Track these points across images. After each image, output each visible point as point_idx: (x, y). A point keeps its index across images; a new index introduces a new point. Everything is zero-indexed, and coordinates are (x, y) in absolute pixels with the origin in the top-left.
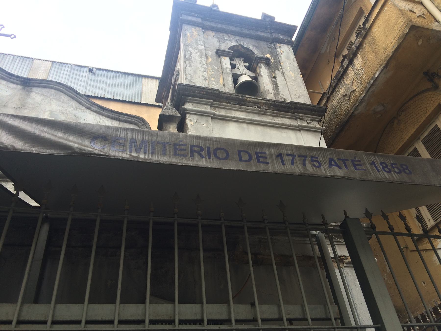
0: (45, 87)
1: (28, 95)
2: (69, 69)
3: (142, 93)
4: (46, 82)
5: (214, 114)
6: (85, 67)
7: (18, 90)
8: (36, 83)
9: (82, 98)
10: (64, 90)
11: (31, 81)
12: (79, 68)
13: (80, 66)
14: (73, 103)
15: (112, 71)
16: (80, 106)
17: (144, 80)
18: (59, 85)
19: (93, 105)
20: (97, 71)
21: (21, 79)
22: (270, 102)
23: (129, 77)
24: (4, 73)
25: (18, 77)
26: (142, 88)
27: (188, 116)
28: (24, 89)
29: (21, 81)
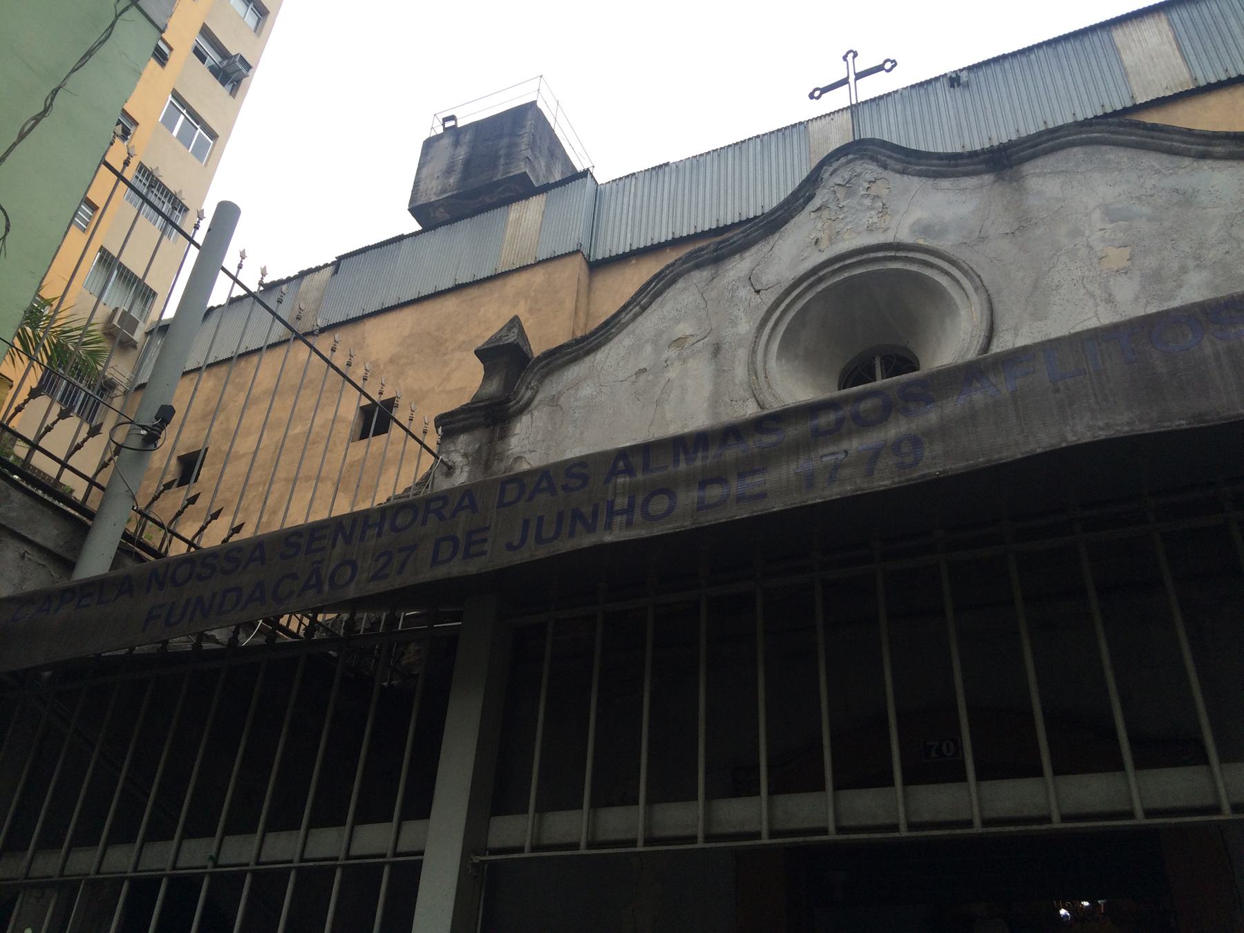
0: (1053, 150)
2: (899, 107)
3: (1125, 75)
4: (1050, 136)
6: (937, 79)
7: (989, 187)
8: (1023, 150)
9: (1171, 136)
10: (1106, 135)
11: (1008, 151)
12: (922, 91)
13: (921, 85)
14: (1151, 160)
15: (1014, 54)
16: (1176, 159)
17: (1118, 34)
18: (1084, 129)
19: (1213, 142)
20: (972, 76)
21: (981, 157)
23: (1069, 46)
24: (935, 162)
25: (973, 154)
26: (1120, 61)
28: (1003, 179)
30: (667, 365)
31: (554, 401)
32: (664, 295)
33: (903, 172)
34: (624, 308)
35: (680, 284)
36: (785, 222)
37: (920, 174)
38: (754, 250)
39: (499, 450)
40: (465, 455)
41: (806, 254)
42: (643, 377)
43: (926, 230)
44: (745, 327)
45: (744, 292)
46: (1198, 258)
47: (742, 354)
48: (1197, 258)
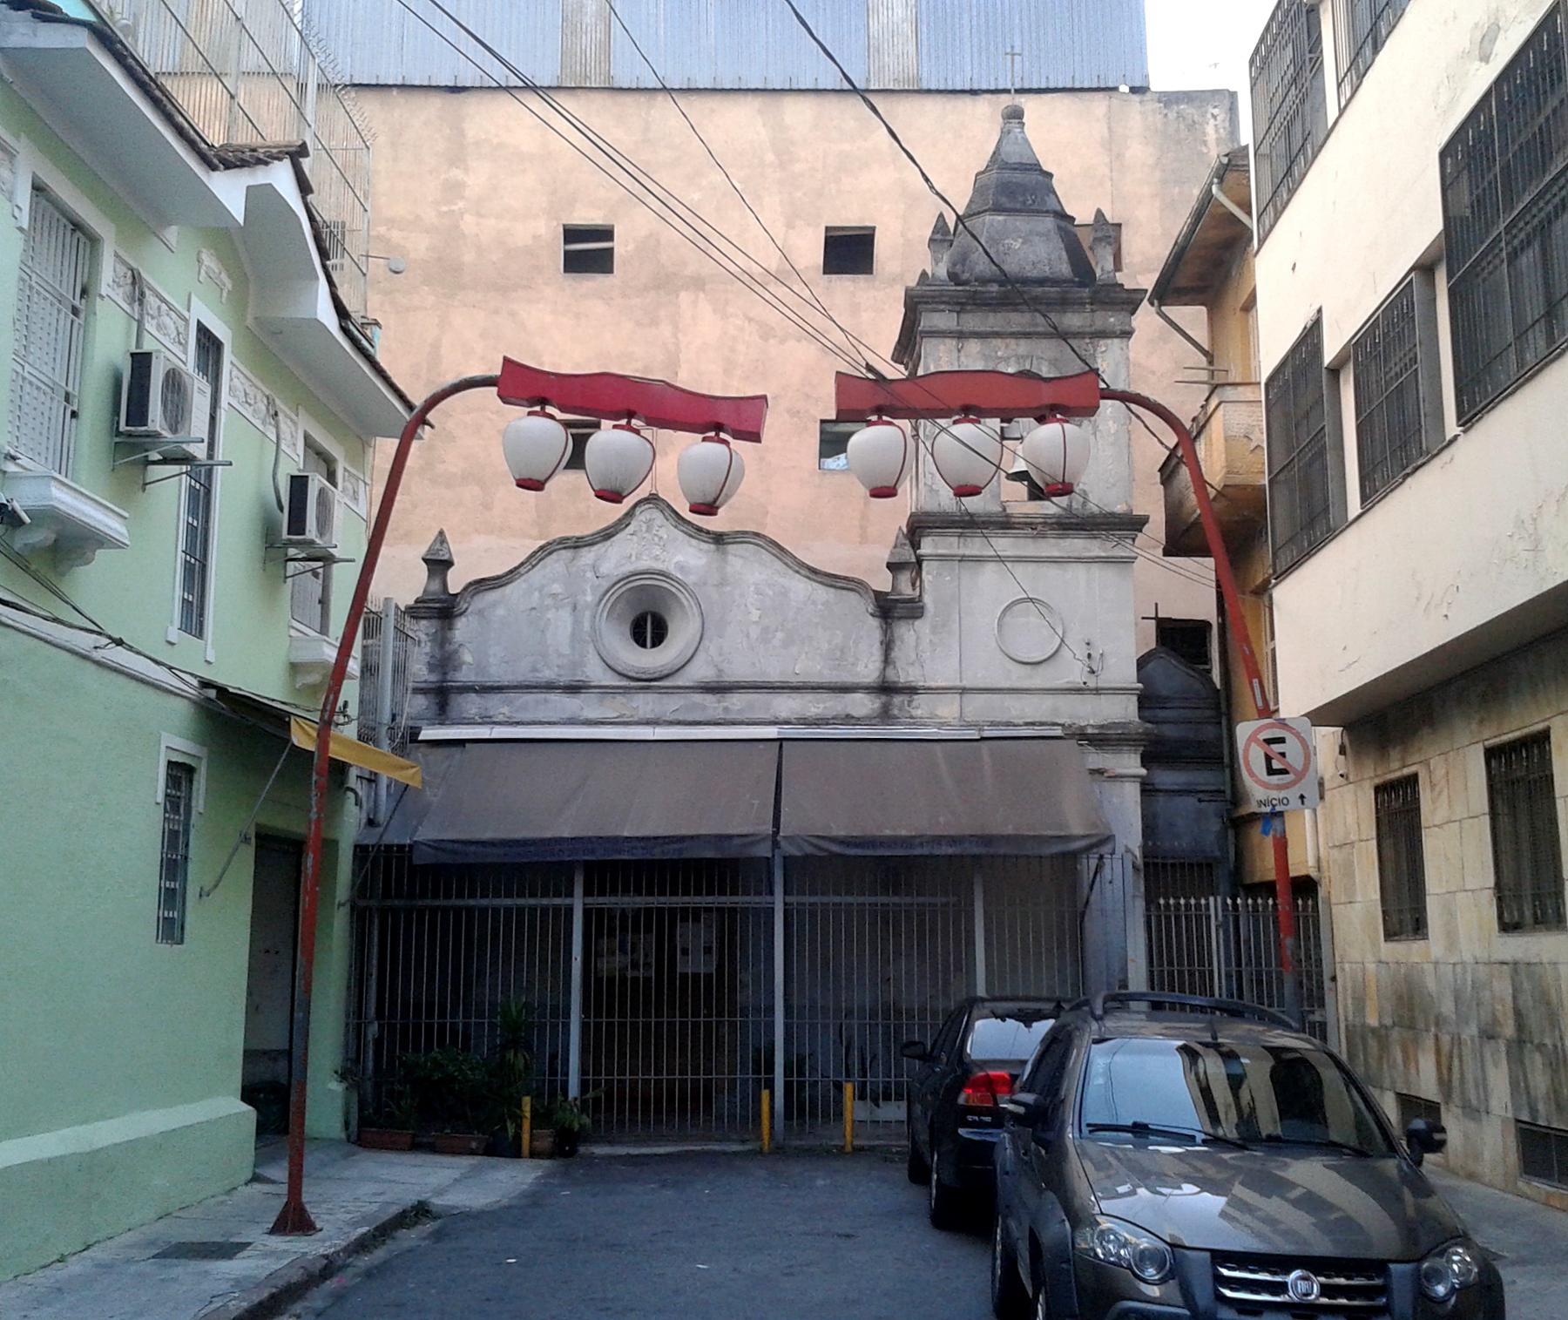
1: (725, 561)
5: (964, 556)
14: (778, 565)
22: (1053, 520)
25: (708, 532)
27: (925, 564)
29: (713, 538)
30: (548, 608)
31: (480, 613)
32: (545, 560)
33: (676, 527)
34: (522, 564)
35: (554, 556)
36: (613, 536)
37: (683, 531)
38: (596, 548)
39: (449, 634)
40: (427, 634)
41: (624, 562)
42: (533, 612)
43: (681, 568)
44: (589, 598)
45: (589, 575)
46: (782, 625)
47: (588, 614)
48: (782, 625)
